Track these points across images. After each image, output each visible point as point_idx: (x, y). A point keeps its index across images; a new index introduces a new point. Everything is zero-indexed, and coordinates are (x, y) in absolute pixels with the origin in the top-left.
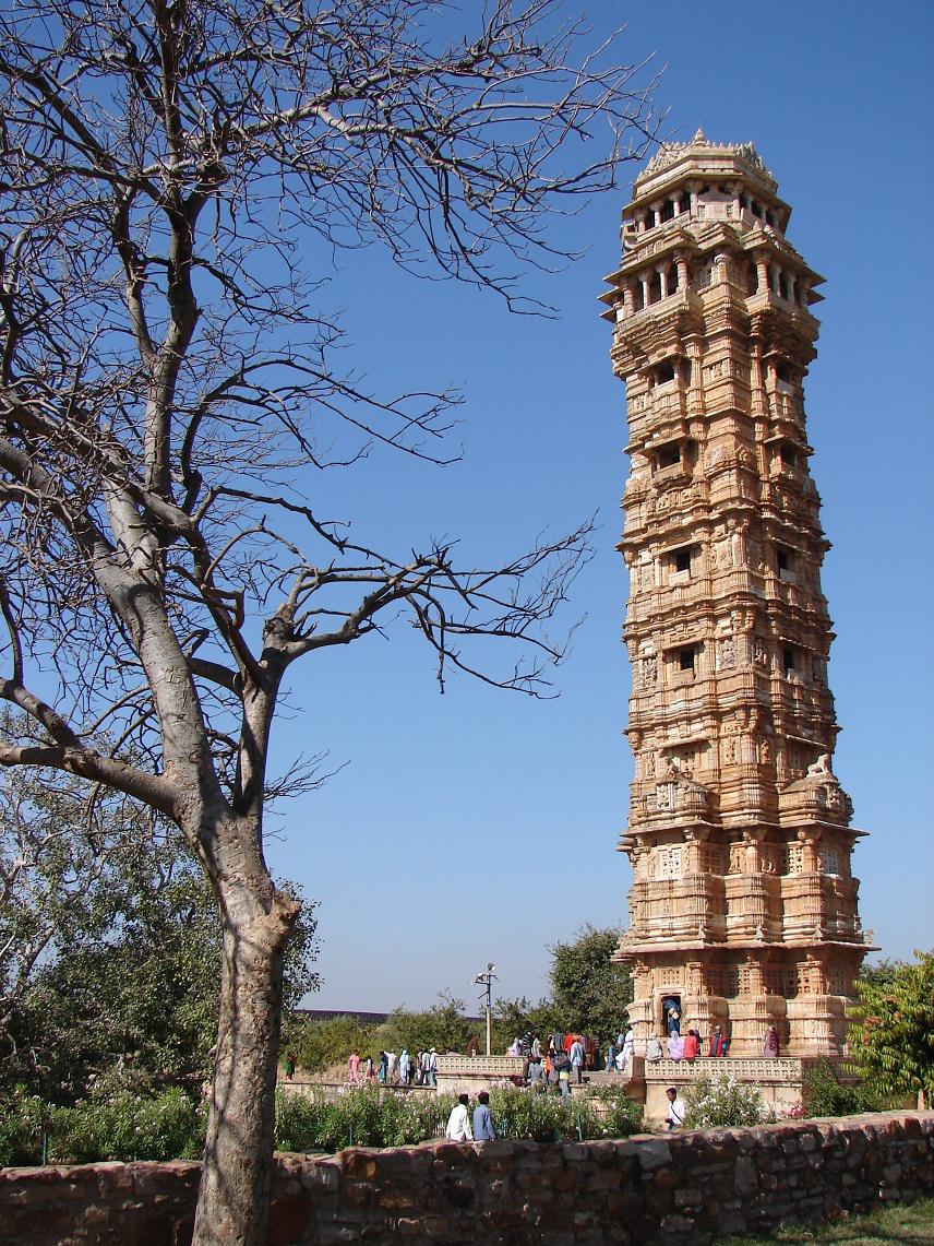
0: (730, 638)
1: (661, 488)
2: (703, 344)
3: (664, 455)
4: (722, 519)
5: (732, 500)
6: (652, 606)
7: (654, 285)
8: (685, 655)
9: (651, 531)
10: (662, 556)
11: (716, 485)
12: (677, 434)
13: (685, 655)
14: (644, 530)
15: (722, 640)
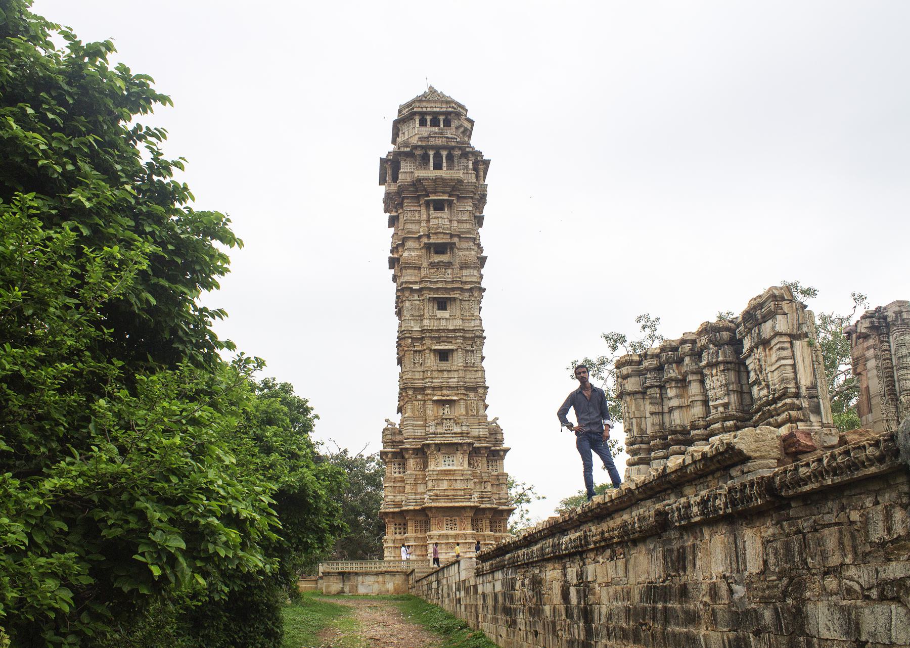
0: (472, 351)
1: (433, 265)
2: (459, 198)
3: (440, 249)
4: (471, 290)
5: (475, 282)
6: (427, 324)
7: (438, 156)
8: (444, 355)
9: (428, 285)
10: (429, 299)
11: (465, 272)
12: (446, 240)
13: (444, 355)
14: (415, 283)
15: (467, 351)
